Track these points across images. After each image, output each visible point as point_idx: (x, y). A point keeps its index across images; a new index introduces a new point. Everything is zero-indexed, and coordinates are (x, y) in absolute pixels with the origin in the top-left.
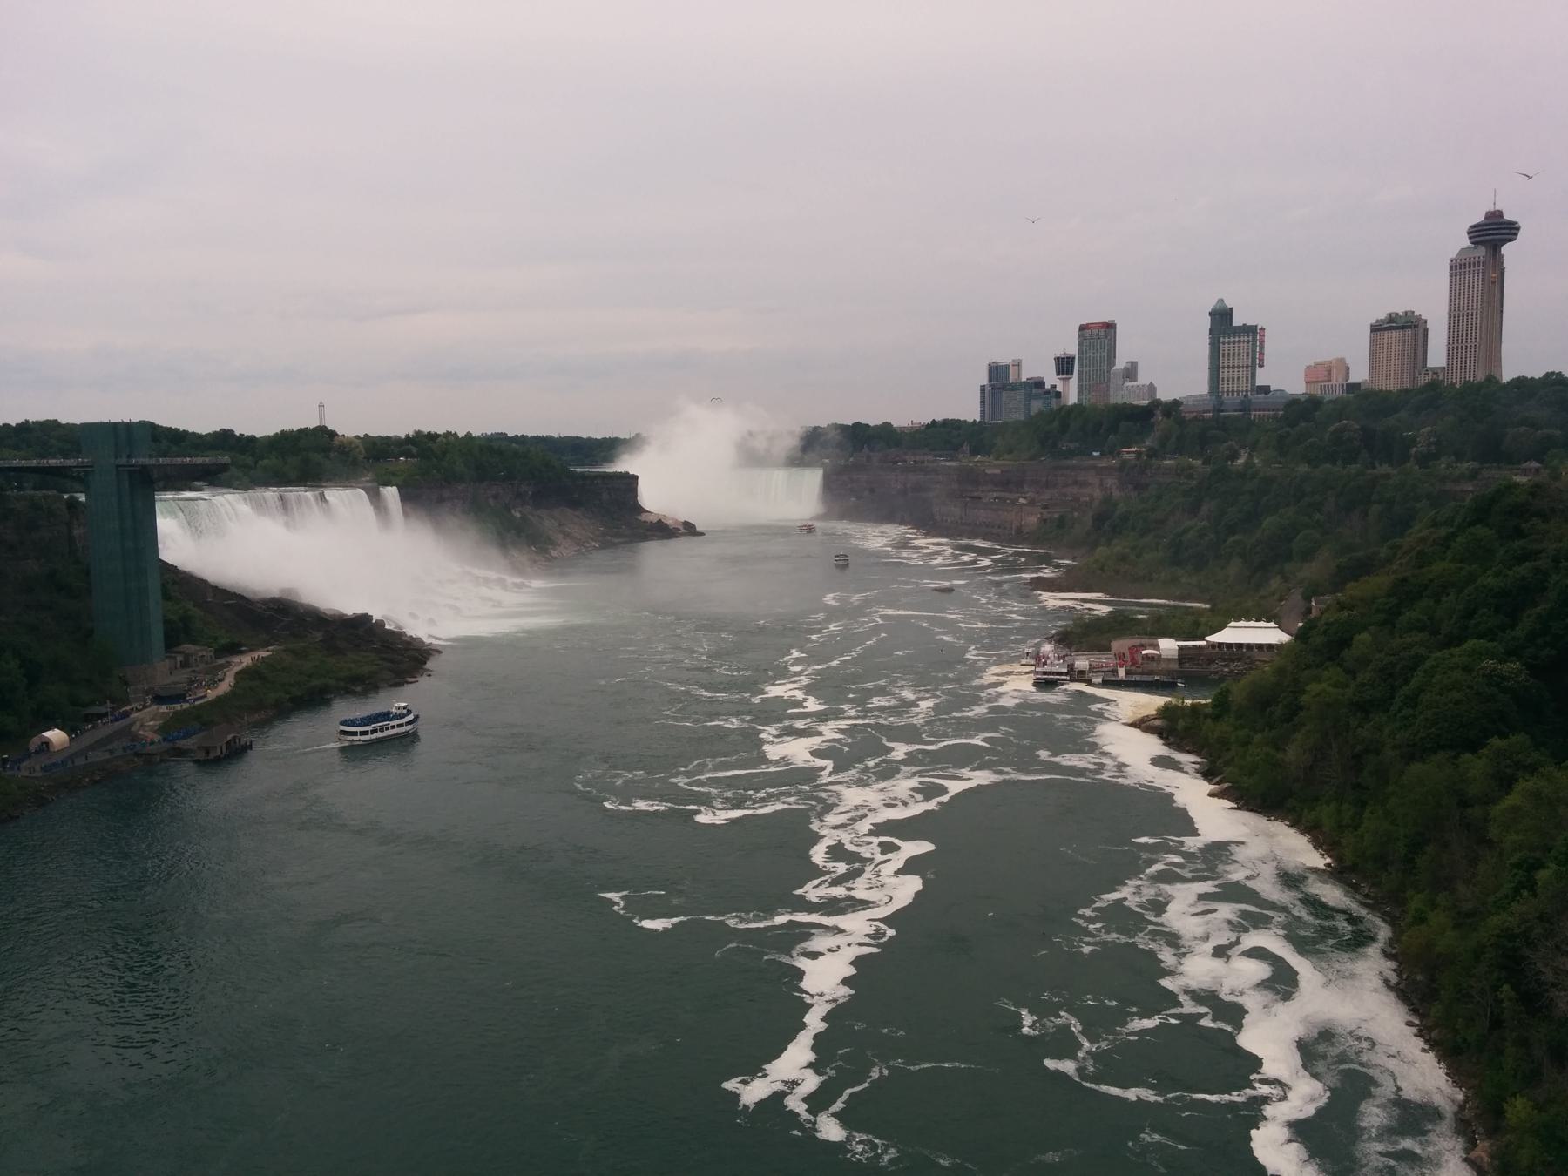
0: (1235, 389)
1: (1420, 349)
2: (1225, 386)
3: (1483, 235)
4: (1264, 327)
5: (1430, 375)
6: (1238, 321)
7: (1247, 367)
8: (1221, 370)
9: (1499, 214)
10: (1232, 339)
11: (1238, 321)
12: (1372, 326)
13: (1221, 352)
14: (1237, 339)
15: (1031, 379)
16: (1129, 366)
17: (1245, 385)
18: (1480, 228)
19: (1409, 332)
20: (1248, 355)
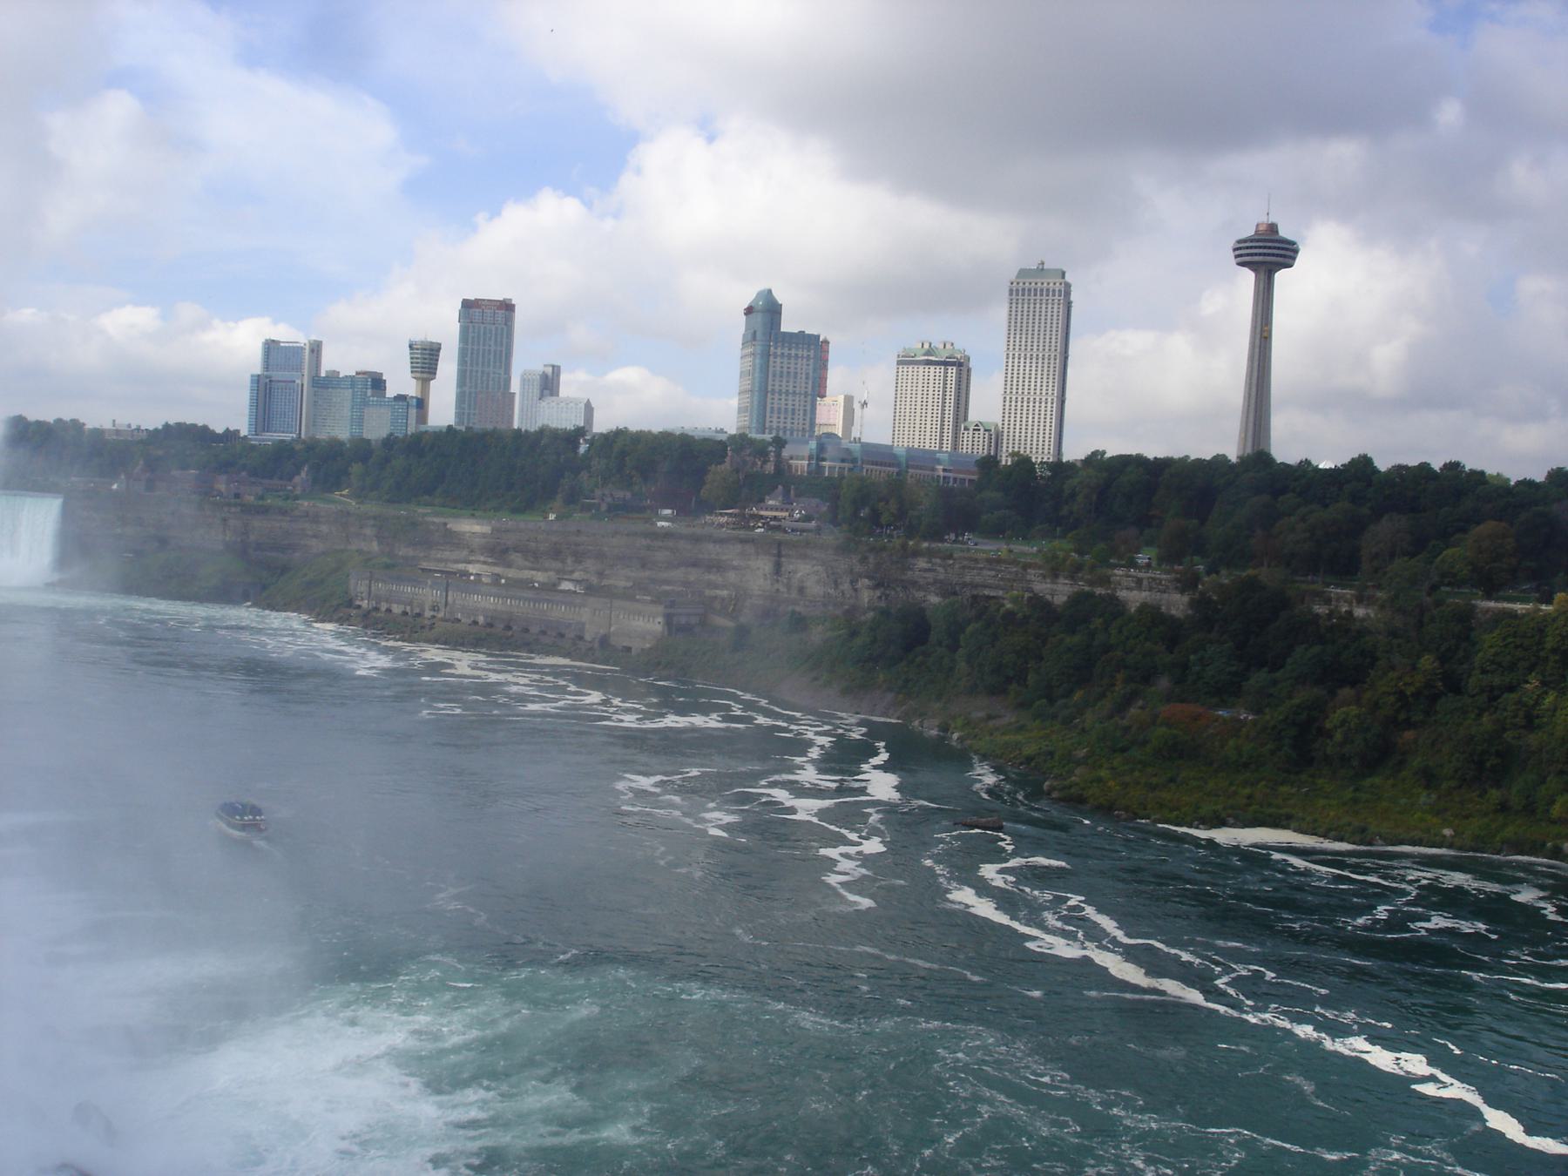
0: (789, 426)
1: (963, 395)
2: (775, 420)
3: (1269, 255)
4: (829, 339)
5: (982, 432)
6: (788, 325)
7: (806, 395)
8: (769, 395)
9: (1273, 228)
11: (788, 325)
13: (771, 369)
15: (365, 373)
16: (549, 370)
17: (801, 421)
18: (1251, 244)
19: (952, 371)
20: (807, 378)
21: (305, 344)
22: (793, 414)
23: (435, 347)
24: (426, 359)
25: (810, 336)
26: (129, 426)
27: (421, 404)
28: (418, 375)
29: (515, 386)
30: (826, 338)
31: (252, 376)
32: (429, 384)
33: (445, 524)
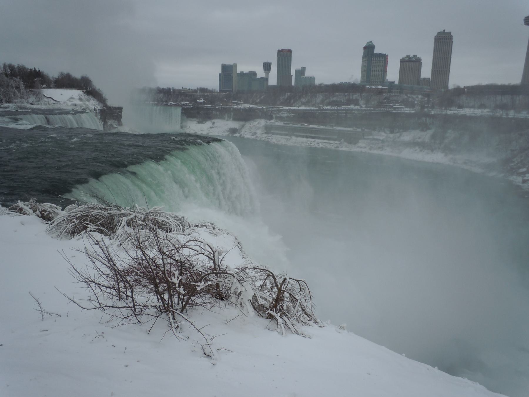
6: (377, 51)
10: (376, 59)
11: (377, 51)
12: (401, 60)
14: (378, 59)
15: (251, 72)
22: (378, 77)
24: (267, 67)
25: (383, 54)
27: (266, 79)
28: (266, 72)
29: (293, 73)
30: (387, 55)
31: (219, 74)
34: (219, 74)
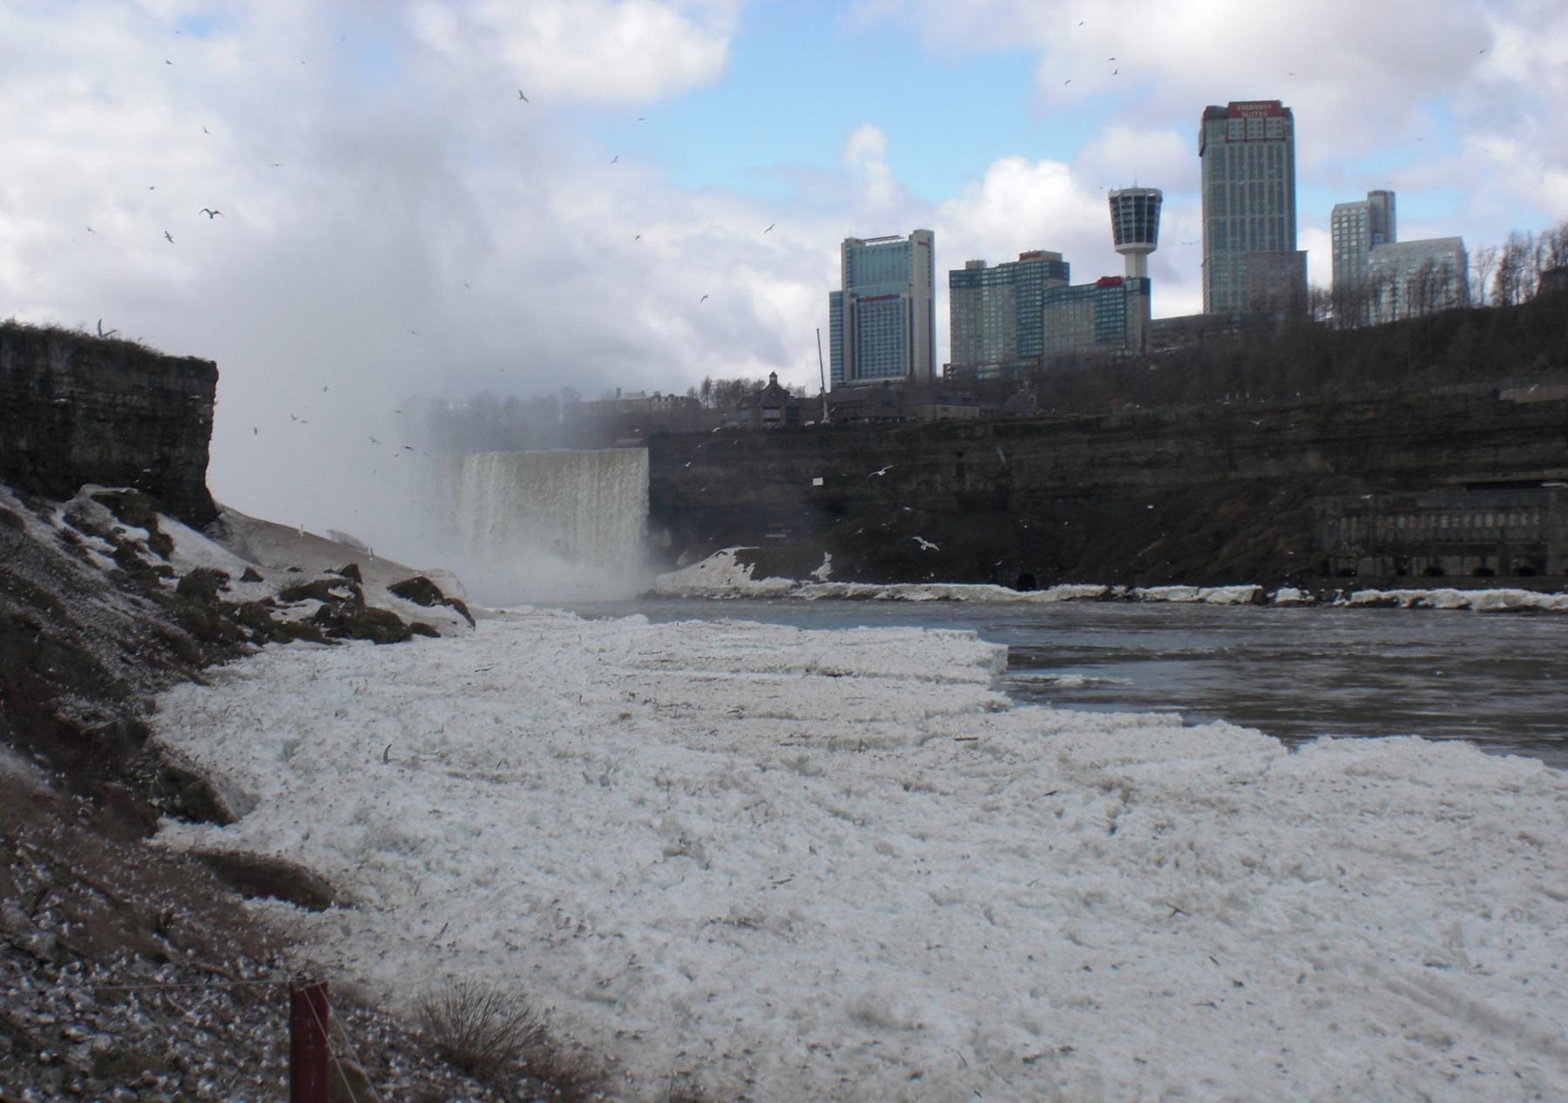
15: (1037, 254)
16: (1379, 200)
21: (910, 237)
23: (1152, 199)
26: (643, 393)
32: (1146, 259)
33: (1496, 393)
34: (832, 295)
